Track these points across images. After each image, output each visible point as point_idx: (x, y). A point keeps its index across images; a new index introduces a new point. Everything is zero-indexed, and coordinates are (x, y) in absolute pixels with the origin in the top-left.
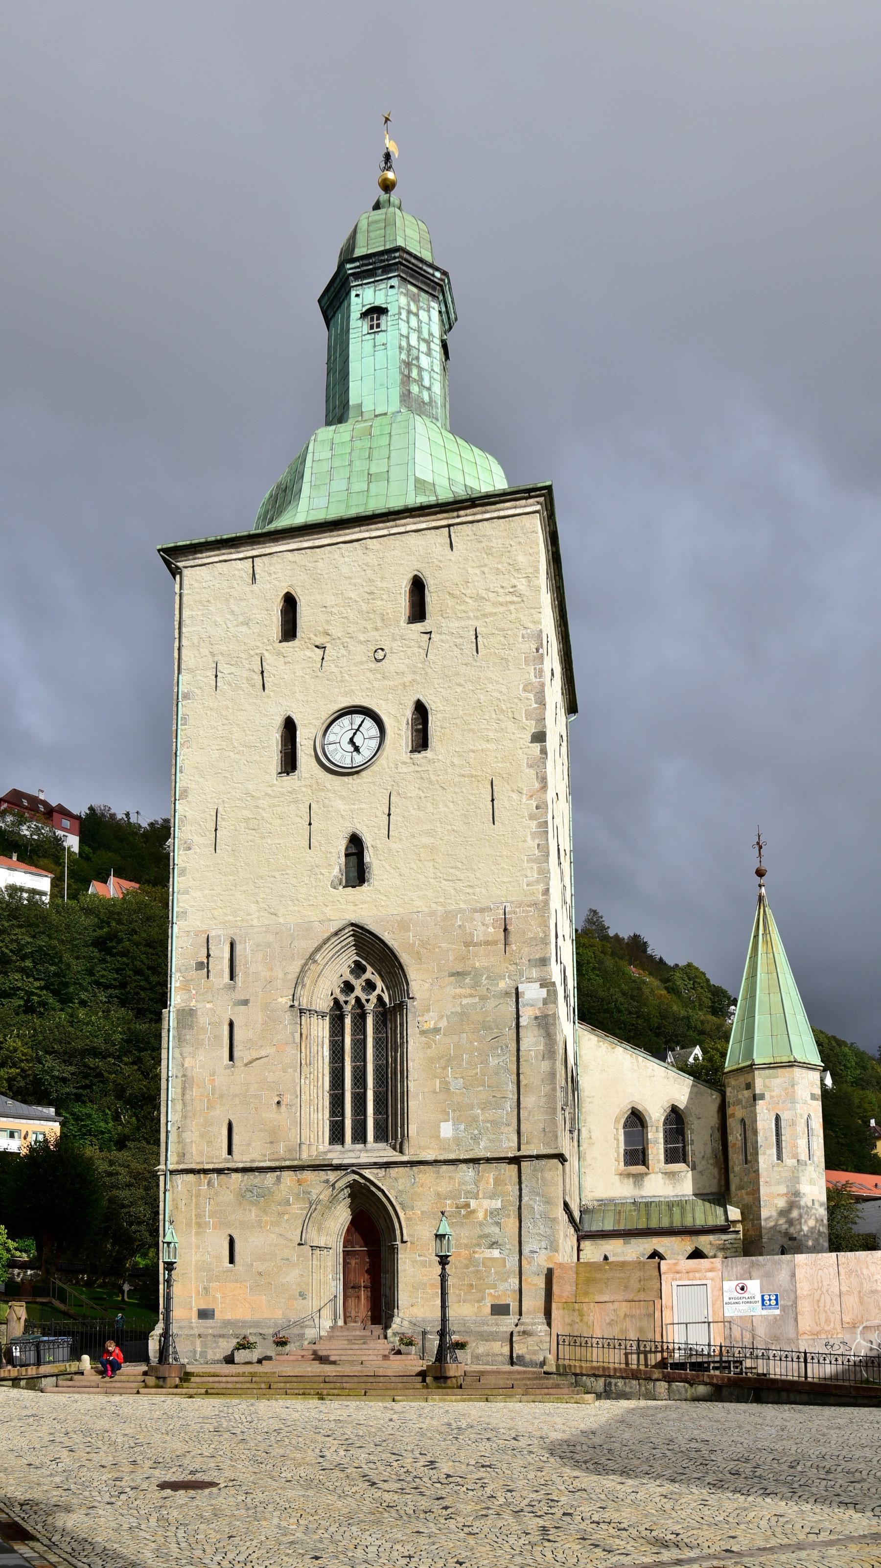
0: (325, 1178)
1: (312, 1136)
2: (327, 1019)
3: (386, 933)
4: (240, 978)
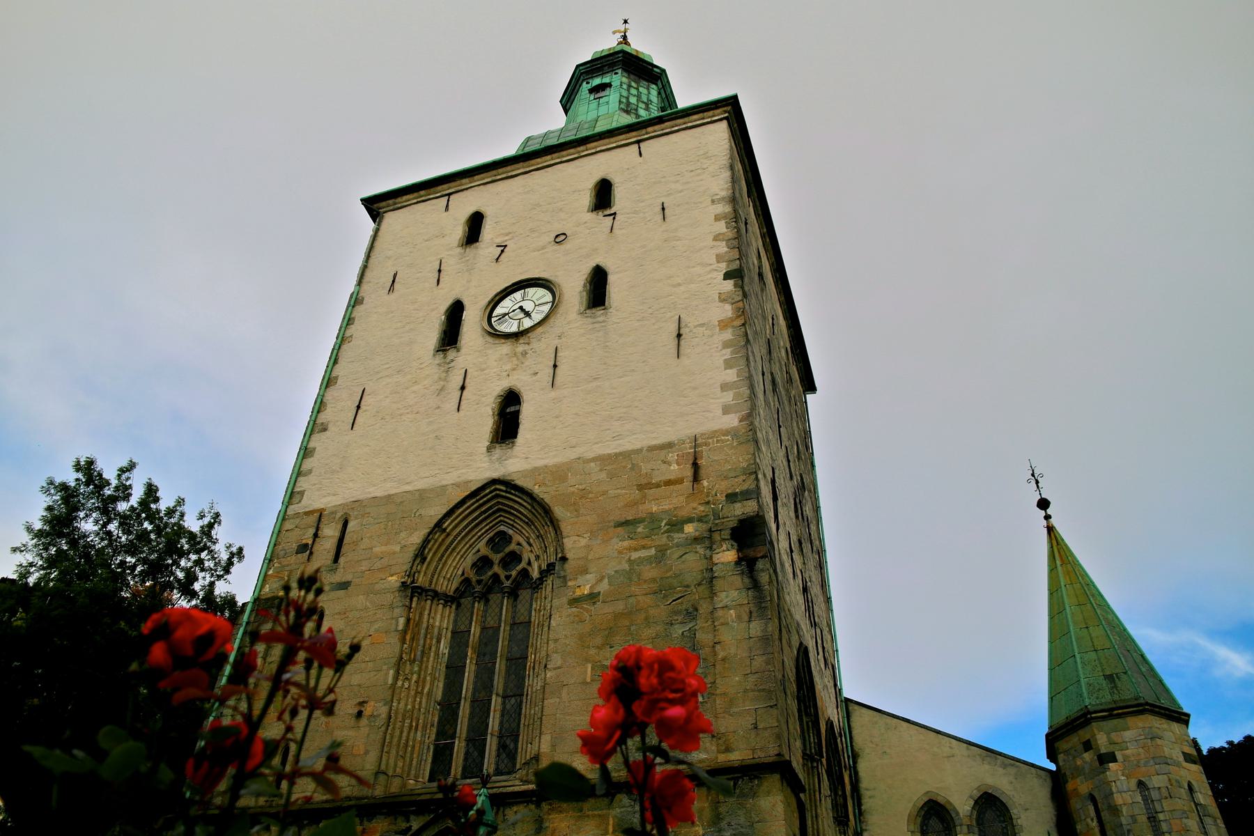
0: (404, 825)
1: (400, 764)
2: (454, 607)
3: (537, 487)
4: (342, 560)
